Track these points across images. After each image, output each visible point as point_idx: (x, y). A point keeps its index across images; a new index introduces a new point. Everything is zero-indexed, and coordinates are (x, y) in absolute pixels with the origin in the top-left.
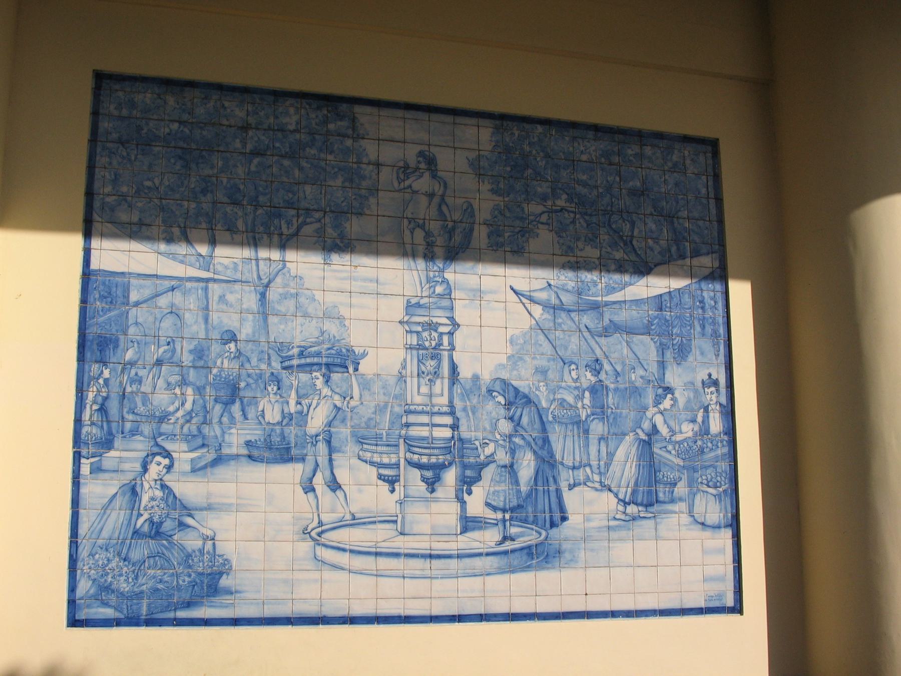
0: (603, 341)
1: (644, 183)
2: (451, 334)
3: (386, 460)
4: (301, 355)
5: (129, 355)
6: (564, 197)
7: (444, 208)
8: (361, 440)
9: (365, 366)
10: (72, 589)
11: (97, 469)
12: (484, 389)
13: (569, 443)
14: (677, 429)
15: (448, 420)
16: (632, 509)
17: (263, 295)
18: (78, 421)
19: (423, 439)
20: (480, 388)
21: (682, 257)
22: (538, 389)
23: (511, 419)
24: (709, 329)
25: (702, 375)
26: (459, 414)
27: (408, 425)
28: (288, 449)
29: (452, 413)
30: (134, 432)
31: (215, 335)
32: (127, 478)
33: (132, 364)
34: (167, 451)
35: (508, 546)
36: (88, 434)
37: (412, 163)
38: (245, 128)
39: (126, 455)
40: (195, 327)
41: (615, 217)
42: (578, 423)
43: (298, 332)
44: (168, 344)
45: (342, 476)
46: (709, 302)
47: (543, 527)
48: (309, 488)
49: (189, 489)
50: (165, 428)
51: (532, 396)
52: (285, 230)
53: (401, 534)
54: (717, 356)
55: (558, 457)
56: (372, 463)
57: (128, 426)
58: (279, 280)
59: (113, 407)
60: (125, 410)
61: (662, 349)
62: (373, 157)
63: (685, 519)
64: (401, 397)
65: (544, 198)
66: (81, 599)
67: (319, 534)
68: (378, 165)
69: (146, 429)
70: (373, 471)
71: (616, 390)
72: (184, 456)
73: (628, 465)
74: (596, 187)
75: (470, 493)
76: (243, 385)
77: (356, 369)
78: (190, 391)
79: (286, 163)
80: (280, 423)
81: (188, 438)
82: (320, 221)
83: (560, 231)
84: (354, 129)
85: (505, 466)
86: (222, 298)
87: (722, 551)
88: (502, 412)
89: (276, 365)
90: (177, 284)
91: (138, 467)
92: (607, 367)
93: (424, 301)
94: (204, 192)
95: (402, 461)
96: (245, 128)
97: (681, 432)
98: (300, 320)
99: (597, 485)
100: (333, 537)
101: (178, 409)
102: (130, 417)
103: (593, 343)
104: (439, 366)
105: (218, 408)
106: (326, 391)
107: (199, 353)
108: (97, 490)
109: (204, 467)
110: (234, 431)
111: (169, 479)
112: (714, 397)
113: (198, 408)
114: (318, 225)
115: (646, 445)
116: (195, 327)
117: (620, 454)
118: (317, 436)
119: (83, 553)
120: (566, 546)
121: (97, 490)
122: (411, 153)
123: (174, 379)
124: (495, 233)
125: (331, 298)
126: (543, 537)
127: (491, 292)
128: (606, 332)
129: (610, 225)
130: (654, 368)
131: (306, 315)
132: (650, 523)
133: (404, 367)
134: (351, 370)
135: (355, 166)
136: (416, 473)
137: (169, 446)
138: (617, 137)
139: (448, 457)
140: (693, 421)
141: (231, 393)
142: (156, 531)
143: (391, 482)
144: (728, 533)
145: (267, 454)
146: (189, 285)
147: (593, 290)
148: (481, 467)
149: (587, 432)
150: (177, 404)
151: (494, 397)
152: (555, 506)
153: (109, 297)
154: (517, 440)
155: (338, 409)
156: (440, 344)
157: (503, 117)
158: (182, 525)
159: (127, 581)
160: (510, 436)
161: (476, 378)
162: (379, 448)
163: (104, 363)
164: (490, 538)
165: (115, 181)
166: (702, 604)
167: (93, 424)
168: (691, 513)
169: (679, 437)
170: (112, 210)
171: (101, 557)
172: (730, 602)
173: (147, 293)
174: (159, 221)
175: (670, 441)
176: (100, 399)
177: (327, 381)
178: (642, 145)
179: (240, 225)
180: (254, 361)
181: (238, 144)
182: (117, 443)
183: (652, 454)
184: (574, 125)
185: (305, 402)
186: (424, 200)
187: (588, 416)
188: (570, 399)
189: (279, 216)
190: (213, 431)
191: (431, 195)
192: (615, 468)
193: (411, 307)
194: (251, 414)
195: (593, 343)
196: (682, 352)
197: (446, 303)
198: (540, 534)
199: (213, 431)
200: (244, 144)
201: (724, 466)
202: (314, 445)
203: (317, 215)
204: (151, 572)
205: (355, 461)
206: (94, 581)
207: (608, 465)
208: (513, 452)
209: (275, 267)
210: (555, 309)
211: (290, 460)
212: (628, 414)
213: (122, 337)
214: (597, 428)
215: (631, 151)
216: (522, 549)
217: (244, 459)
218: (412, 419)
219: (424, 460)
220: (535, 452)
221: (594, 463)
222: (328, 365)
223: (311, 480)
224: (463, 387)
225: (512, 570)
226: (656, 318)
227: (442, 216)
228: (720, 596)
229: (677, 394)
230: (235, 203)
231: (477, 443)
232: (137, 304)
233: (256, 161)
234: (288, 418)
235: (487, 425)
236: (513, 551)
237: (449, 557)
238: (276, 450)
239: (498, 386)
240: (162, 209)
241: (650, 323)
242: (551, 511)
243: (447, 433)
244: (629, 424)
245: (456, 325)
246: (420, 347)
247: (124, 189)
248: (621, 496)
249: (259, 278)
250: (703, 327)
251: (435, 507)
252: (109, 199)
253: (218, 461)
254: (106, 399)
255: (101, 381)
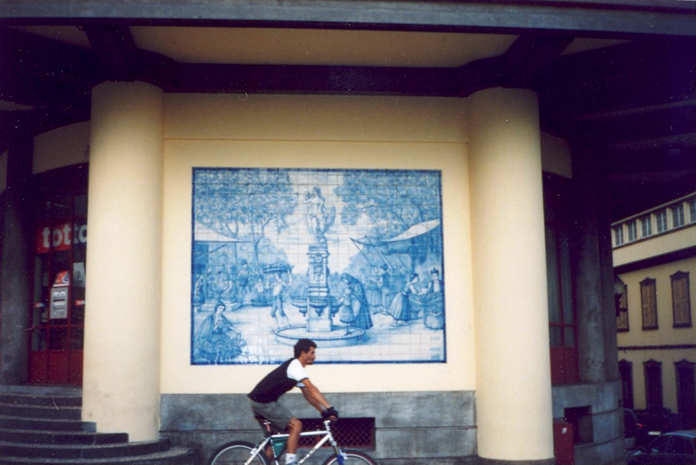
0: (388, 257)
1: (407, 192)
2: (326, 257)
3: (302, 305)
4: (270, 268)
5: (209, 270)
6: (373, 200)
7: (324, 209)
8: (293, 298)
9: (294, 271)
10: (192, 352)
11: (199, 311)
12: (339, 278)
13: (374, 296)
14: (419, 290)
15: (325, 290)
16: (400, 322)
17: (256, 246)
18: (192, 295)
19: (316, 297)
20: (337, 278)
21: (423, 221)
22: (361, 276)
23: (350, 288)
24: (434, 250)
25: (431, 269)
26: (330, 287)
27: (310, 292)
28: (266, 302)
29: (327, 287)
30: (212, 297)
31: (239, 262)
32: (210, 314)
33: (210, 273)
34: (222, 303)
35: (349, 336)
36: (196, 299)
37: (311, 193)
38: (247, 184)
39: (209, 305)
40: (232, 260)
41: (394, 207)
42: (377, 289)
43: (269, 259)
44: (223, 266)
45: (286, 311)
46: (435, 239)
47: (363, 329)
48: (274, 316)
49: (231, 317)
50: (223, 295)
51: (359, 280)
52: (264, 222)
53: (308, 331)
54: (438, 260)
55: (369, 302)
56: (297, 306)
57: (210, 295)
58: (262, 241)
59: (204, 289)
60: (208, 290)
61: (414, 259)
62: (296, 191)
63: (422, 326)
64: (307, 282)
65: (364, 202)
66: (196, 355)
67: (278, 332)
68: (298, 194)
69: (216, 296)
70: (297, 309)
71: (393, 276)
72: (229, 305)
73: (398, 305)
74: (386, 195)
75: (334, 316)
76: (249, 279)
77: (291, 272)
78: (231, 282)
79: (263, 196)
80: (263, 293)
81: (231, 299)
82: (276, 217)
83: (371, 214)
84: (288, 181)
85: (347, 306)
86: (241, 249)
87: (438, 338)
88: (347, 286)
89: (261, 272)
90: (225, 245)
91: (213, 309)
92: (390, 267)
93: (316, 245)
94: (233, 210)
95: (308, 306)
96: (247, 184)
97: (421, 292)
98: (270, 255)
99: (385, 313)
100: (281, 333)
101: (226, 289)
102: (210, 292)
103: (384, 258)
104: (322, 269)
105: (241, 288)
106: (280, 280)
107: (234, 269)
108: (200, 318)
109: (237, 309)
110: (247, 296)
111: (225, 314)
112: (436, 278)
113: (234, 288)
114: (275, 219)
115: (406, 297)
116: (232, 260)
117: (395, 300)
118: (277, 296)
119: (196, 340)
120: (372, 336)
121: (200, 318)
122: (311, 189)
123: (225, 278)
124: (344, 217)
125: (280, 246)
126: (362, 333)
127: (343, 240)
128: (389, 253)
129: (392, 211)
130: (409, 267)
131: (271, 253)
132: (407, 328)
133: (309, 270)
134: (289, 272)
135: (289, 195)
136: (313, 310)
137: (224, 302)
138: (396, 174)
139: (326, 303)
140: (427, 287)
141: (245, 282)
142: (220, 332)
143: (304, 313)
144: (441, 332)
145: (259, 304)
146: (229, 244)
147: (384, 237)
148: (338, 307)
149: (381, 292)
150: (226, 287)
151: (343, 281)
152: (368, 321)
153: (201, 250)
154: (353, 296)
155: (284, 287)
156: (322, 261)
157: (347, 171)
158: (229, 330)
159: (210, 349)
160: (350, 295)
161: (336, 274)
162: (300, 301)
163: (200, 273)
164: (341, 333)
165: (202, 207)
166: (429, 359)
167: (197, 295)
168: (425, 324)
169: (420, 294)
170: (201, 218)
171: (202, 341)
172: (442, 358)
173: (215, 248)
174: (218, 221)
175: (416, 295)
176: (200, 287)
177: (280, 276)
178: (407, 176)
179: (247, 221)
180: (253, 270)
181: (245, 191)
182: (206, 301)
183: (408, 301)
184: (377, 171)
185: (272, 285)
186: (316, 207)
187: (382, 286)
188: (374, 280)
189: (261, 216)
190: (239, 296)
191: (318, 205)
192: (393, 306)
193: (311, 248)
194: (253, 289)
195: (384, 258)
196: (423, 260)
197: (324, 245)
198: (362, 331)
199: (239, 296)
200: (247, 191)
201: (440, 305)
202: (275, 300)
203: (275, 215)
204: (219, 346)
205: (291, 306)
206: (200, 349)
207: (390, 305)
208: (351, 301)
209: (260, 236)
210: (368, 245)
211: (267, 305)
212: (399, 285)
213: (206, 264)
214: (386, 291)
215: (402, 179)
216: (354, 337)
217: (251, 306)
218: (312, 289)
219: (317, 304)
220: (360, 301)
221: (384, 304)
222: (280, 271)
223: (274, 312)
224: (331, 277)
225: (351, 345)
226: (411, 246)
227: (323, 212)
228: (438, 356)
229: (420, 277)
230: (245, 212)
231: (337, 298)
232: (211, 252)
233: (252, 196)
234: (266, 291)
235: (341, 292)
236: (351, 338)
237: (326, 340)
238: (262, 302)
239: (345, 276)
240: (219, 217)
241: (409, 249)
242: (366, 323)
243: (325, 294)
244: (399, 289)
245: (328, 254)
246: (315, 263)
247: (205, 210)
248: (395, 317)
249: (254, 240)
250: (432, 249)
251: (321, 322)
252: (201, 215)
253: (241, 307)
254: (202, 286)
255: (200, 280)
